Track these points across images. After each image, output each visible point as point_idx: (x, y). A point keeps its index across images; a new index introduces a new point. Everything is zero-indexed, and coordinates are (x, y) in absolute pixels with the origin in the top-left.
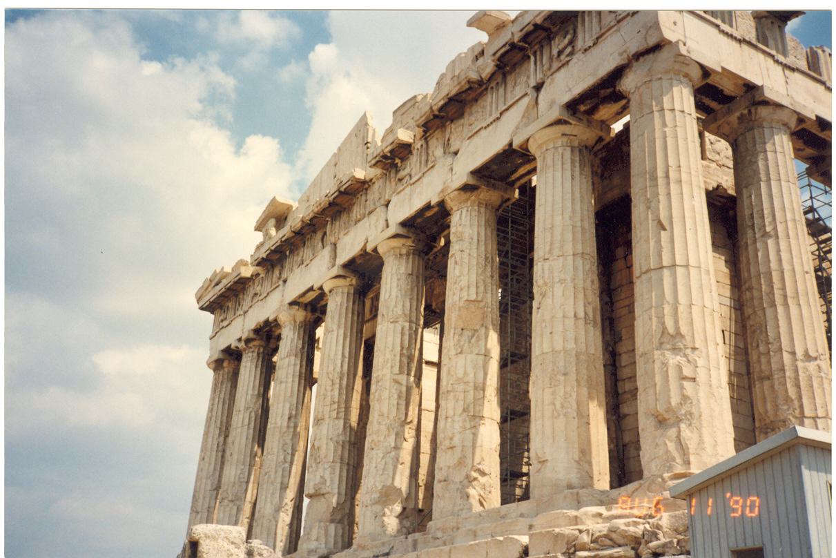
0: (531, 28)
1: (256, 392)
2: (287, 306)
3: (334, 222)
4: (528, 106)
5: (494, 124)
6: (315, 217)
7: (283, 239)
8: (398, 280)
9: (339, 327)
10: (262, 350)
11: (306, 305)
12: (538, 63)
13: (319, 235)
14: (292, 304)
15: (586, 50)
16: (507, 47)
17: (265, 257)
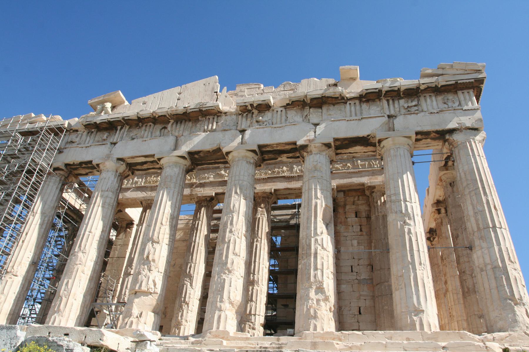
0: (396, 89)
1: (52, 205)
2: (115, 159)
3: (179, 124)
4: (383, 124)
5: (357, 121)
6: (165, 116)
7: (126, 118)
8: (248, 176)
9: (175, 188)
10: (63, 179)
11: (128, 164)
12: (391, 106)
13: (159, 127)
14: (119, 159)
15: (431, 113)
16: (377, 90)
17: (98, 122)
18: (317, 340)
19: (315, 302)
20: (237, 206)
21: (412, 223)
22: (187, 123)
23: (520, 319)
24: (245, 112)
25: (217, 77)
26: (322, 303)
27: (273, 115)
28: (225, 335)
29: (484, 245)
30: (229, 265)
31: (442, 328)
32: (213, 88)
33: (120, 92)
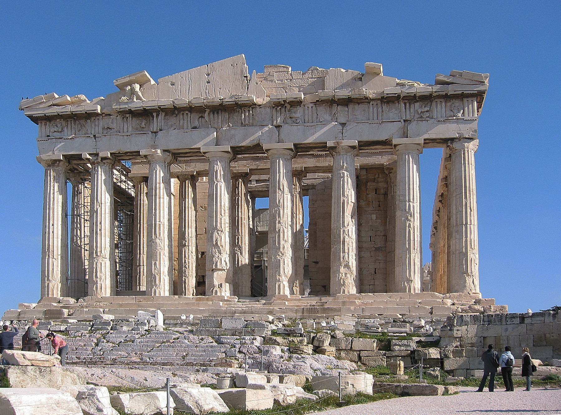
12: (408, 111)
13: (195, 116)
18: (345, 300)
19: (344, 275)
20: (281, 201)
21: (412, 220)
22: (223, 113)
23: (467, 285)
24: (278, 106)
25: (243, 55)
26: (348, 275)
27: (304, 111)
28: (285, 298)
29: (458, 236)
30: (281, 250)
31: (423, 290)
32: (242, 71)
33: (146, 73)
